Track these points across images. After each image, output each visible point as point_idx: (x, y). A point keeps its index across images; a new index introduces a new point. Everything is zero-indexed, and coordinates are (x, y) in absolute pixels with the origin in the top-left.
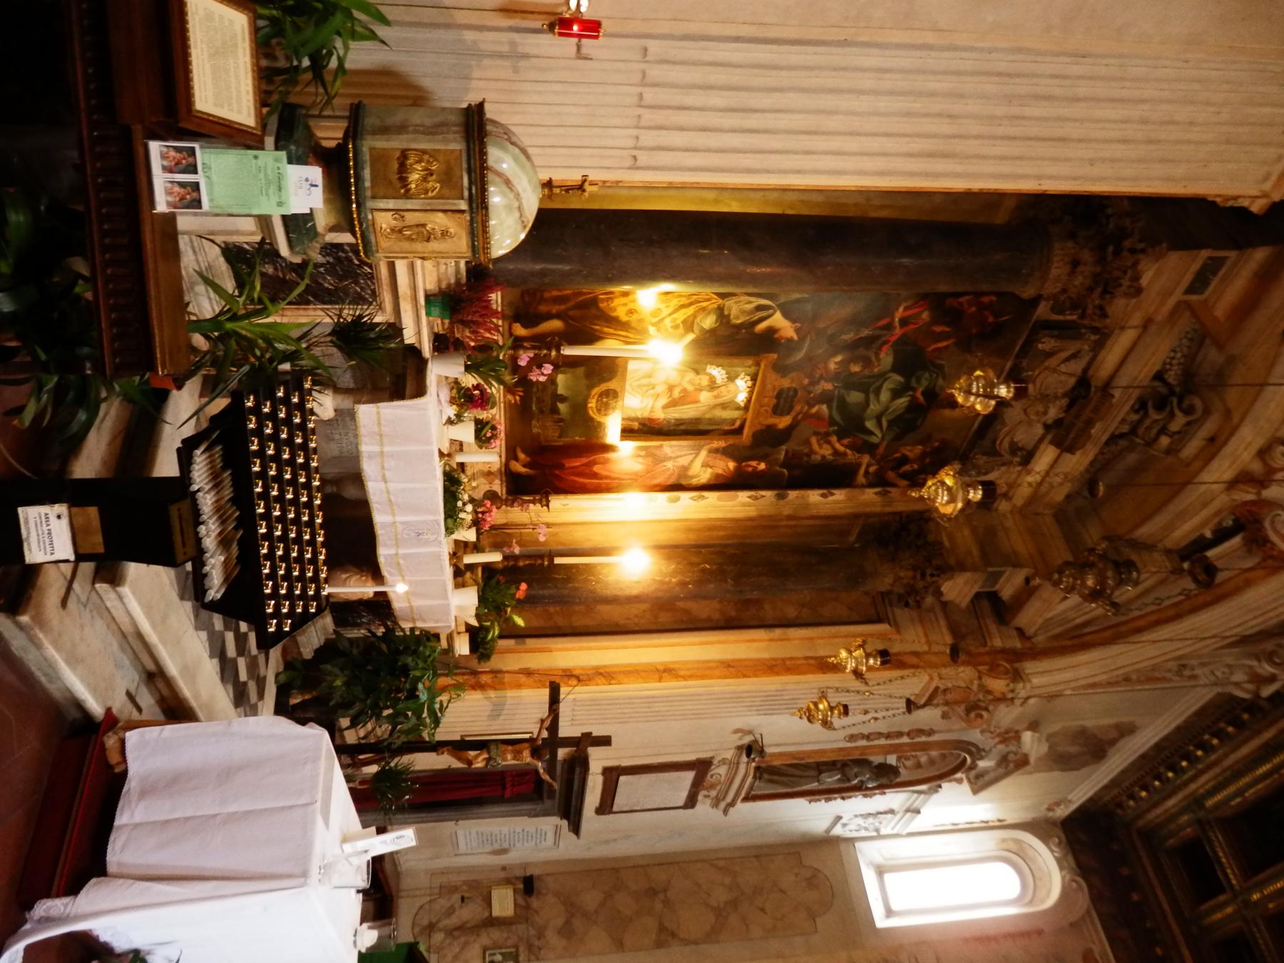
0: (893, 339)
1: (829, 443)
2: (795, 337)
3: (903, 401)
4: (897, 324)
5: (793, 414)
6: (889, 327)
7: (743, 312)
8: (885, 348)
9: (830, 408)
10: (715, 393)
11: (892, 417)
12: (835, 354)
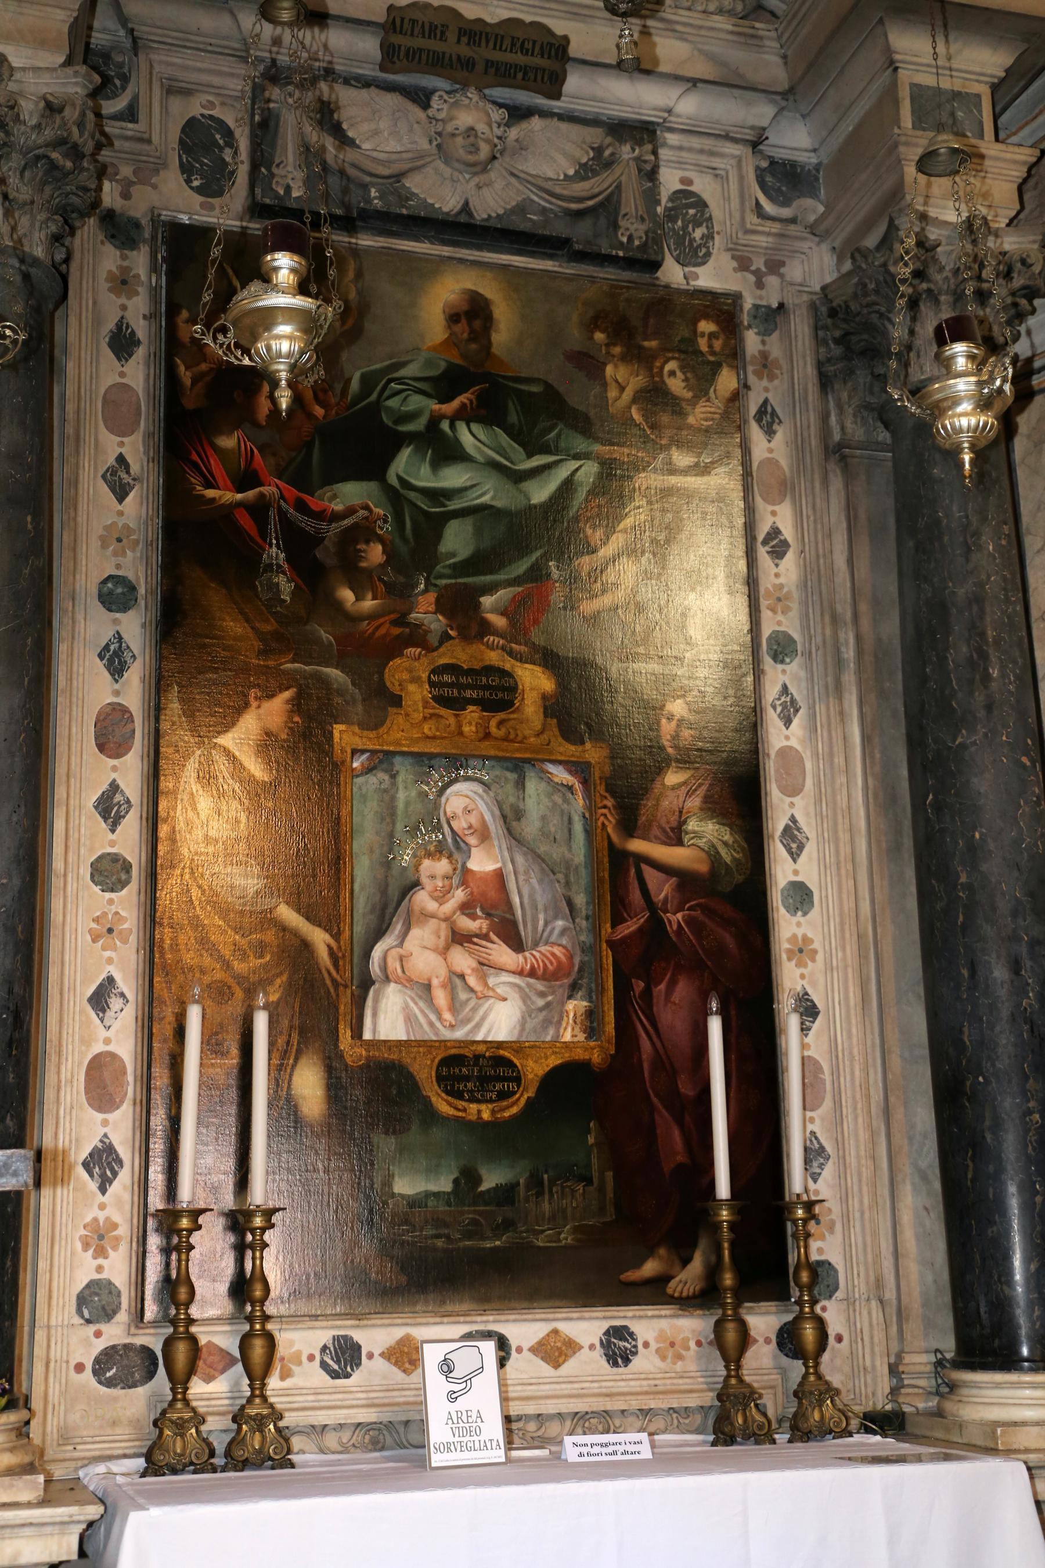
0: (291, 492)
2: (287, 694)
3: (469, 438)
4: (251, 494)
6: (259, 510)
8: (314, 503)
9: (490, 589)
10: (472, 841)
12: (338, 606)
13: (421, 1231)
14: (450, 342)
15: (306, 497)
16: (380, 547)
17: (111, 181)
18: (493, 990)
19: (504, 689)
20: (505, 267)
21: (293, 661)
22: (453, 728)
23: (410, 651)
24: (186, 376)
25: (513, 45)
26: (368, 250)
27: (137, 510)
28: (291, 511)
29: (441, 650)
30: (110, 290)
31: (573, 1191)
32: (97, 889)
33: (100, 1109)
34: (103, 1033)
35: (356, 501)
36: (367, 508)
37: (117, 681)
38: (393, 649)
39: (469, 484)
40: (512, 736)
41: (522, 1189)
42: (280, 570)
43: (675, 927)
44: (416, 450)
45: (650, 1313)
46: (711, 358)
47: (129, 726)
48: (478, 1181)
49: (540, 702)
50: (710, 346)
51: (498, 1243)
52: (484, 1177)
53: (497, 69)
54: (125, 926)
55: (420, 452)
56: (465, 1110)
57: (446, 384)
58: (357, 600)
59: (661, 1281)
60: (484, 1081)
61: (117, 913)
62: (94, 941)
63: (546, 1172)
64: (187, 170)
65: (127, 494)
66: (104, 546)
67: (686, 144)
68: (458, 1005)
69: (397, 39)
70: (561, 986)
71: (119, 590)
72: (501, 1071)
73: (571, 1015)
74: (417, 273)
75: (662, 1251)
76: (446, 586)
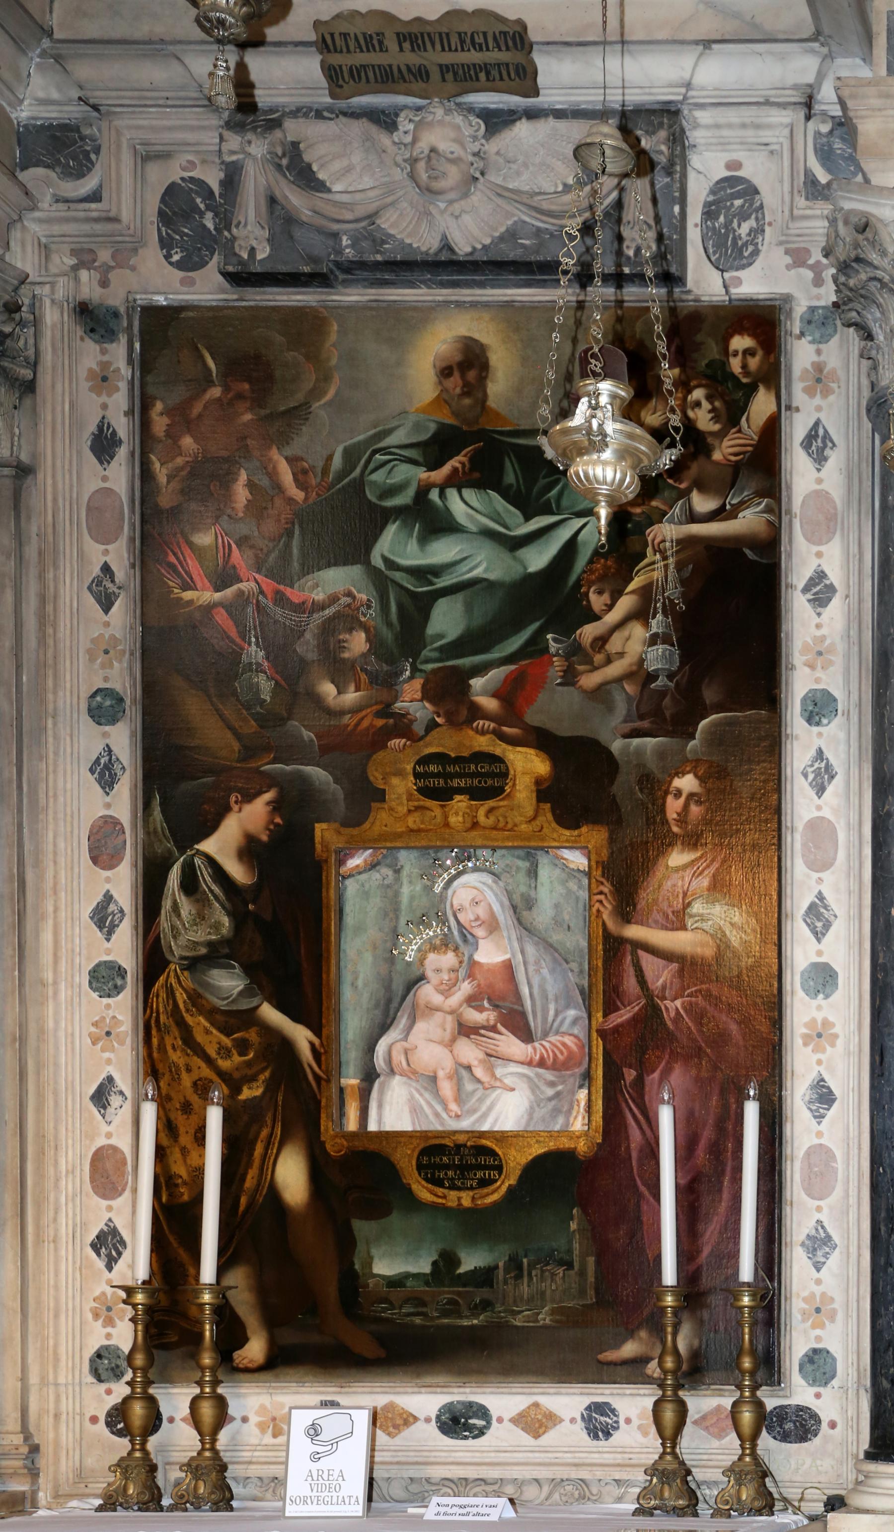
1: (602, 641)
2: (268, 796)
3: (461, 506)
4: (229, 592)
5: (500, 749)
7: (200, 917)
8: (294, 594)
9: (479, 670)
11: (512, 514)
13: (401, 1308)
14: (441, 401)
15: (288, 591)
16: (363, 635)
17: (89, 269)
19: (492, 775)
20: (508, 305)
21: (274, 761)
22: (439, 819)
23: (396, 743)
24: (161, 472)
25: (462, 42)
26: (350, 308)
27: (120, 619)
28: (271, 605)
29: (428, 738)
30: (91, 389)
31: (553, 1275)
32: (95, 995)
33: (104, 1197)
34: (105, 1128)
35: (340, 588)
36: (349, 594)
37: (108, 794)
38: (377, 741)
39: (458, 557)
40: (501, 825)
41: (501, 1272)
42: (259, 669)
43: (673, 1014)
44: (405, 524)
46: (745, 380)
47: (121, 837)
48: (457, 1263)
49: (534, 788)
50: (744, 366)
52: (463, 1260)
53: (455, 74)
54: (123, 1029)
55: (407, 526)
56: (444, 1197)
57: (436, 448)
58: (339, 693)
59: (640, 1361)
61: (114, 1017)
62: (94, 1044)
63: (526, 1256)
64: (166, 244)
65: (112, 604)
66: (92, 660)
67: (721, 120)
69: (336, 59)
71: (108, 703)
72: (482, 1160)
74: (403, 324)
75: (643, 1334)
76: (434, 671)
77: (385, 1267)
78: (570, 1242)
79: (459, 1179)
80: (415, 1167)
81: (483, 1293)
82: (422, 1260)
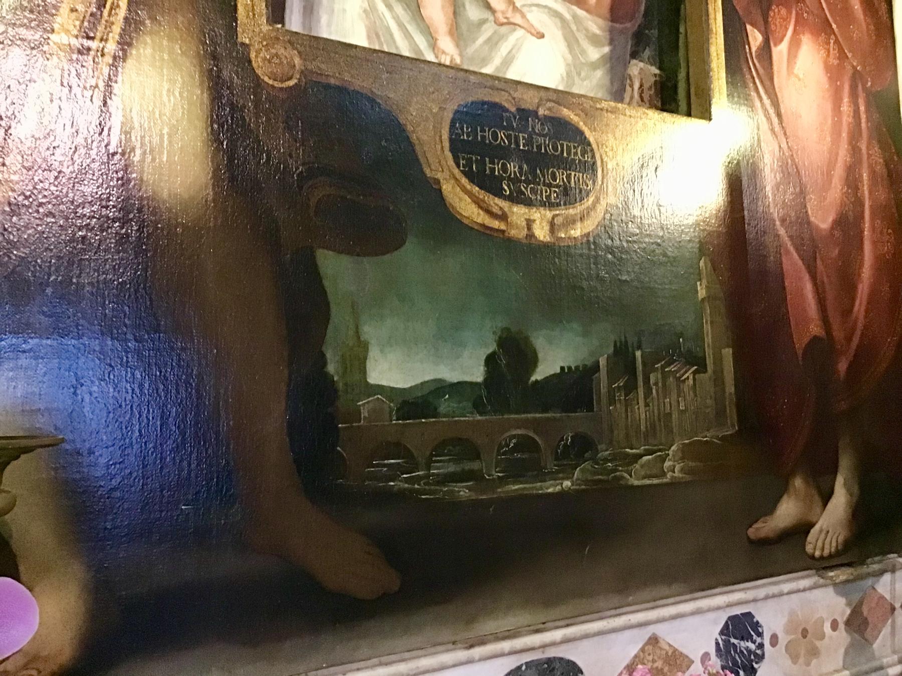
18: (523, 16)
31: (680, 381)
45: (786, 587)
48: (530, 360)
51: (567, 483)
52: (540, 355)
56: (503, 217)
60: (540, 162)
68: (464, 27)
70: (622, 32)
73: (637, 86)
75: (798, 482)
77: (393, 369)
78: (700, 317)
79: (527, 182)
80: (447, 144)
81: (577, 422)
82: (466, 354)
